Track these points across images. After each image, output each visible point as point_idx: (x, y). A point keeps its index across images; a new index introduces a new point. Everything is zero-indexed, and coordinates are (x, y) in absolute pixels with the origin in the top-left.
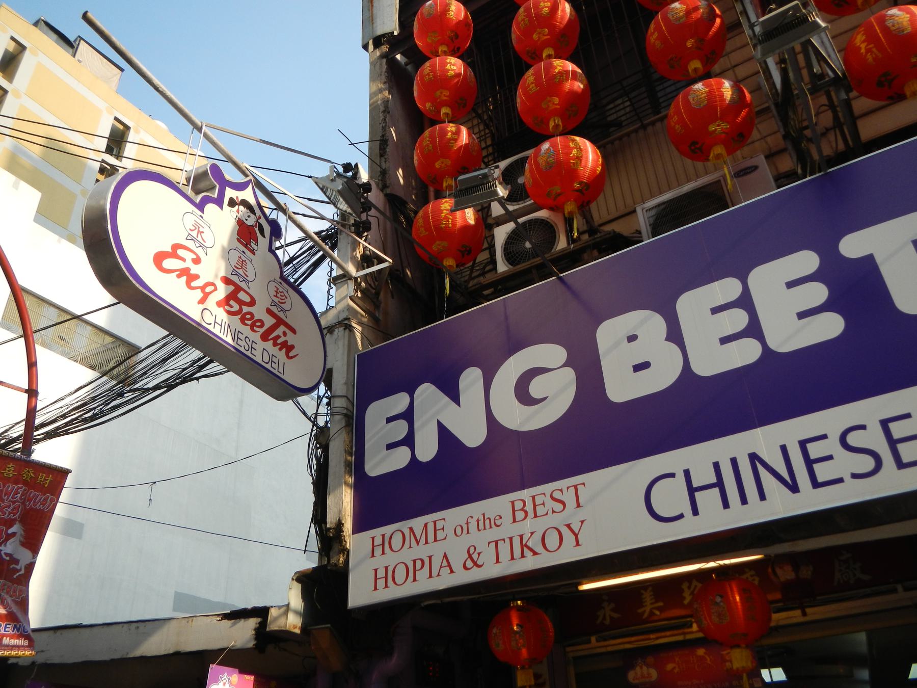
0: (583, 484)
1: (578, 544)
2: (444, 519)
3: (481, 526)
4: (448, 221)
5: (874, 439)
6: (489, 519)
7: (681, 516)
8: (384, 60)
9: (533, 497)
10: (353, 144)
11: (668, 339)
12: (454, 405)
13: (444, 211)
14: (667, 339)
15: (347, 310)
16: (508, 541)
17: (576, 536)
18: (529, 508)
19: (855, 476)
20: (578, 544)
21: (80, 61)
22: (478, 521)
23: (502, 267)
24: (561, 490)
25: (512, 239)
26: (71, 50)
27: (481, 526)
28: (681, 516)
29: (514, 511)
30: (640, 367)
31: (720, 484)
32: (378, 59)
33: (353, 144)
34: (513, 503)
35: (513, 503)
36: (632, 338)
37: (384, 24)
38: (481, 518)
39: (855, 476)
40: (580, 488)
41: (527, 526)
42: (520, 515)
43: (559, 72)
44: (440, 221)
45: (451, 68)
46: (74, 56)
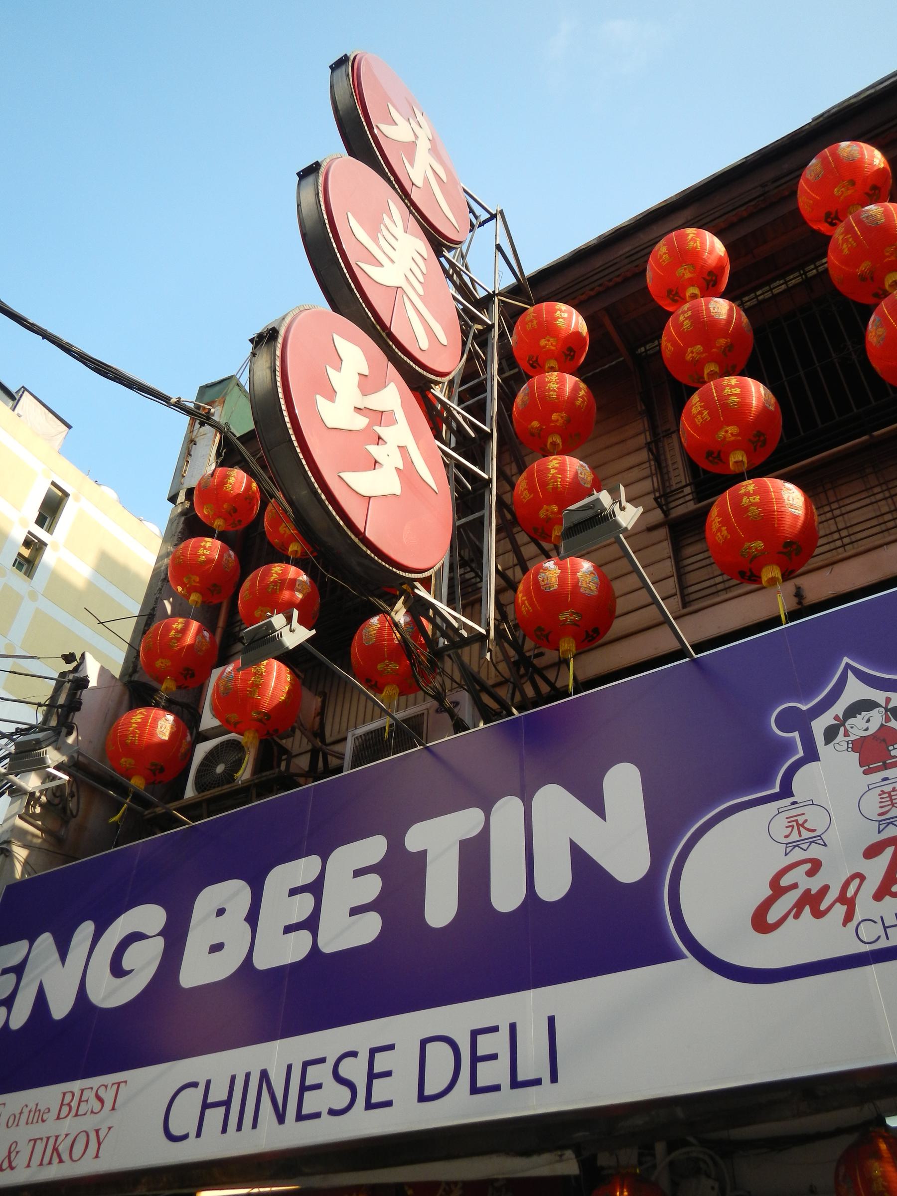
0: (126, 1082)
1: (97, 1156)
2: (4, 1104)
3: (30, 1121)
4: (135, 737)
5: (355, 1070)
6: (40, 1111)
7: (185, 1137)
8: (183, 519)
9: (82, 1091)
10: (102, 623)
11: (246, 919)
12: (60, 963)
13: (134, 725)
14: (246, 919)
15: (11, 831)
16: (45, 1140)
17: (99, 1144)
18: (74, 1104)
19: (332, 1112)
20: (97, 1156)
21: (19, 416)
22: (30, 1111)
23: (190, 792)
24: (106, 1087)
25: (212, 758)
26: (11, 403)
27: (30, 1121)
28: (185, 1137)
29: (62, 1104)
30: (217, 948)
31: (227, 1103)
32: (178, 516)
33: (102, 623)
34: (64, 1094)
35: (64, 1094)
36: (221, 912)
37: (192, 476)
38: (33, 1109)
39: (332, 1112)
40: (122, 1085)
41: (69, 1126)
42: (65, 1109)
43: (275, 582)
44: (126, 736)
45: (203, 552)
46: (14, 410)
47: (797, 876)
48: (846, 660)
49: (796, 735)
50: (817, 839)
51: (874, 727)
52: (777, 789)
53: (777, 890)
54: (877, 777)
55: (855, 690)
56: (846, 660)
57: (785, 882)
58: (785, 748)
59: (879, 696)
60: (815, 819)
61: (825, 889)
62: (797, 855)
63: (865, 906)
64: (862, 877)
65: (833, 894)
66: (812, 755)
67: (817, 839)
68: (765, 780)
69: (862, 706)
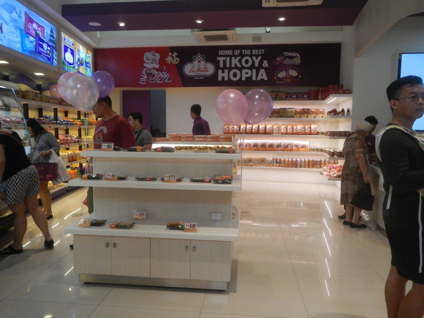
47: (192, 69)
48: (199, 54)
49: (194, 59)
50: (194, 67)
52: (192, 63)
53: (191, 70)
54: (199, 63)
55: (199, 56)
56: (199, 54)
57: (192, 69)
58: (193, 59)
59: (200, 57)
60: (194, 66)
61: (194, 71)
62: (193, 68)
63: (196, 72)
64: (196, 70)
65: (194, 71)
66: (195, 61)
67: (194, 67)
68: (192, 62)
69: (199, 58)
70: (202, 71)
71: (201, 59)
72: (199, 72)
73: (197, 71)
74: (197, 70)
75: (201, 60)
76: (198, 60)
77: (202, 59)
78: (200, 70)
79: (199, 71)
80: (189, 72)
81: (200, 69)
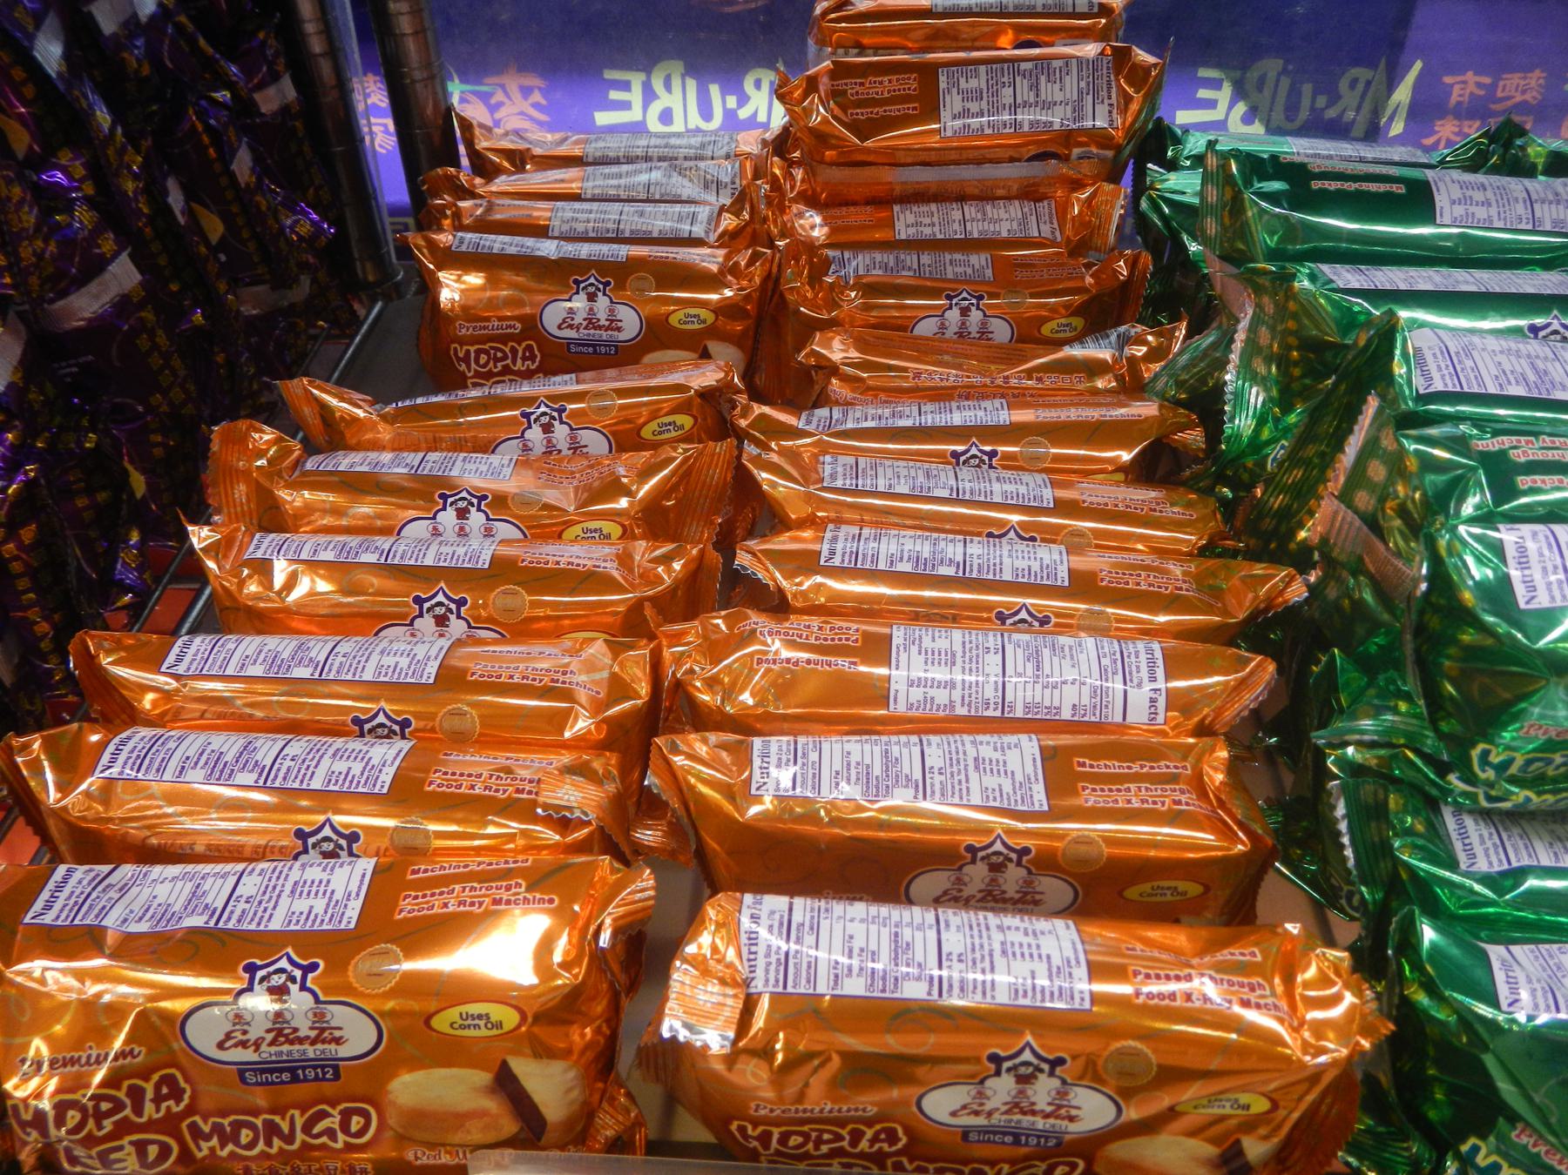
51: (281, 981)
59: (289, 967)
61: (248, 1041)
64: (263, 1039)
69: (278, 971)
70: (301, 1041)
71: (293, 979)
72: (285, 1048)
73: (271, 1044)
74: (270, 1037)
75: (289, 984)
76: (273, 983)
77: (299, 979)
78: (286, 1036)
79: (282, 1039)
80: (221, 1046)
81: (286, 1031)
